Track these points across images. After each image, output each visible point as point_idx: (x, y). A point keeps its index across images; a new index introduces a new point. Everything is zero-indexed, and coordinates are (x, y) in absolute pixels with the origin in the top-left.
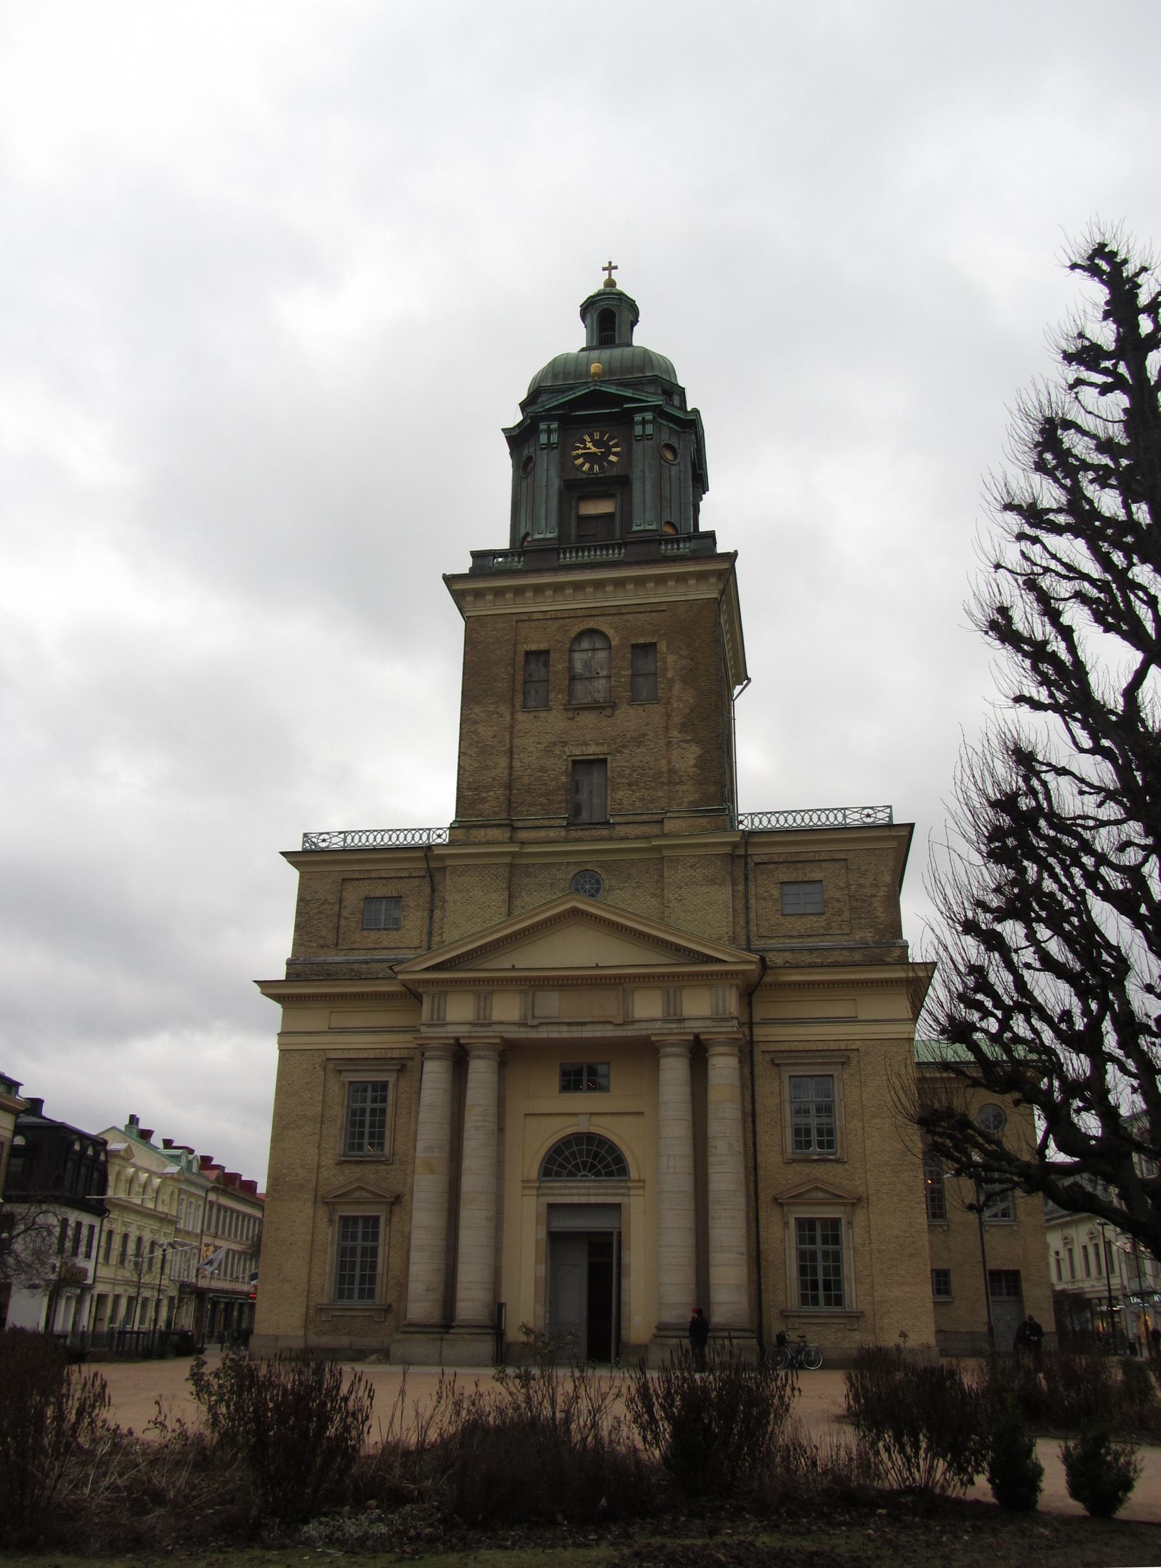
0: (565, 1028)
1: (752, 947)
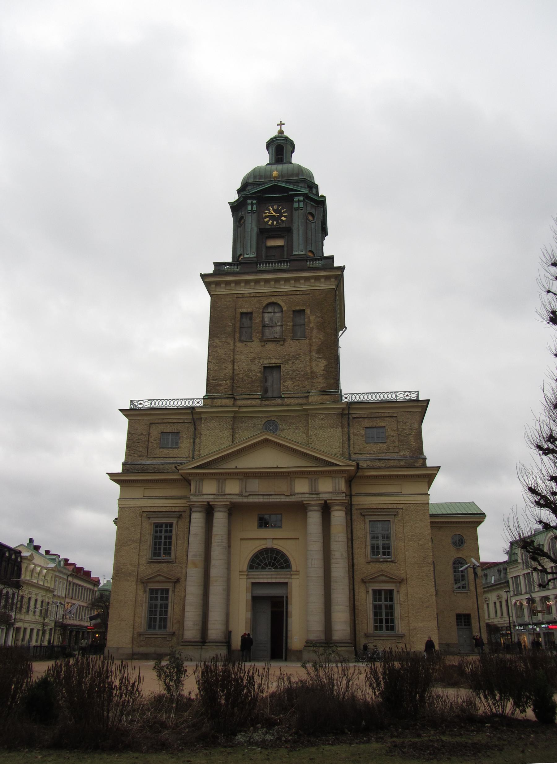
0: (261, 497)
1: (351, 458)
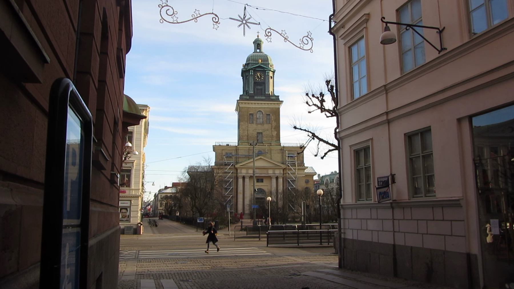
0: (259, 174)
